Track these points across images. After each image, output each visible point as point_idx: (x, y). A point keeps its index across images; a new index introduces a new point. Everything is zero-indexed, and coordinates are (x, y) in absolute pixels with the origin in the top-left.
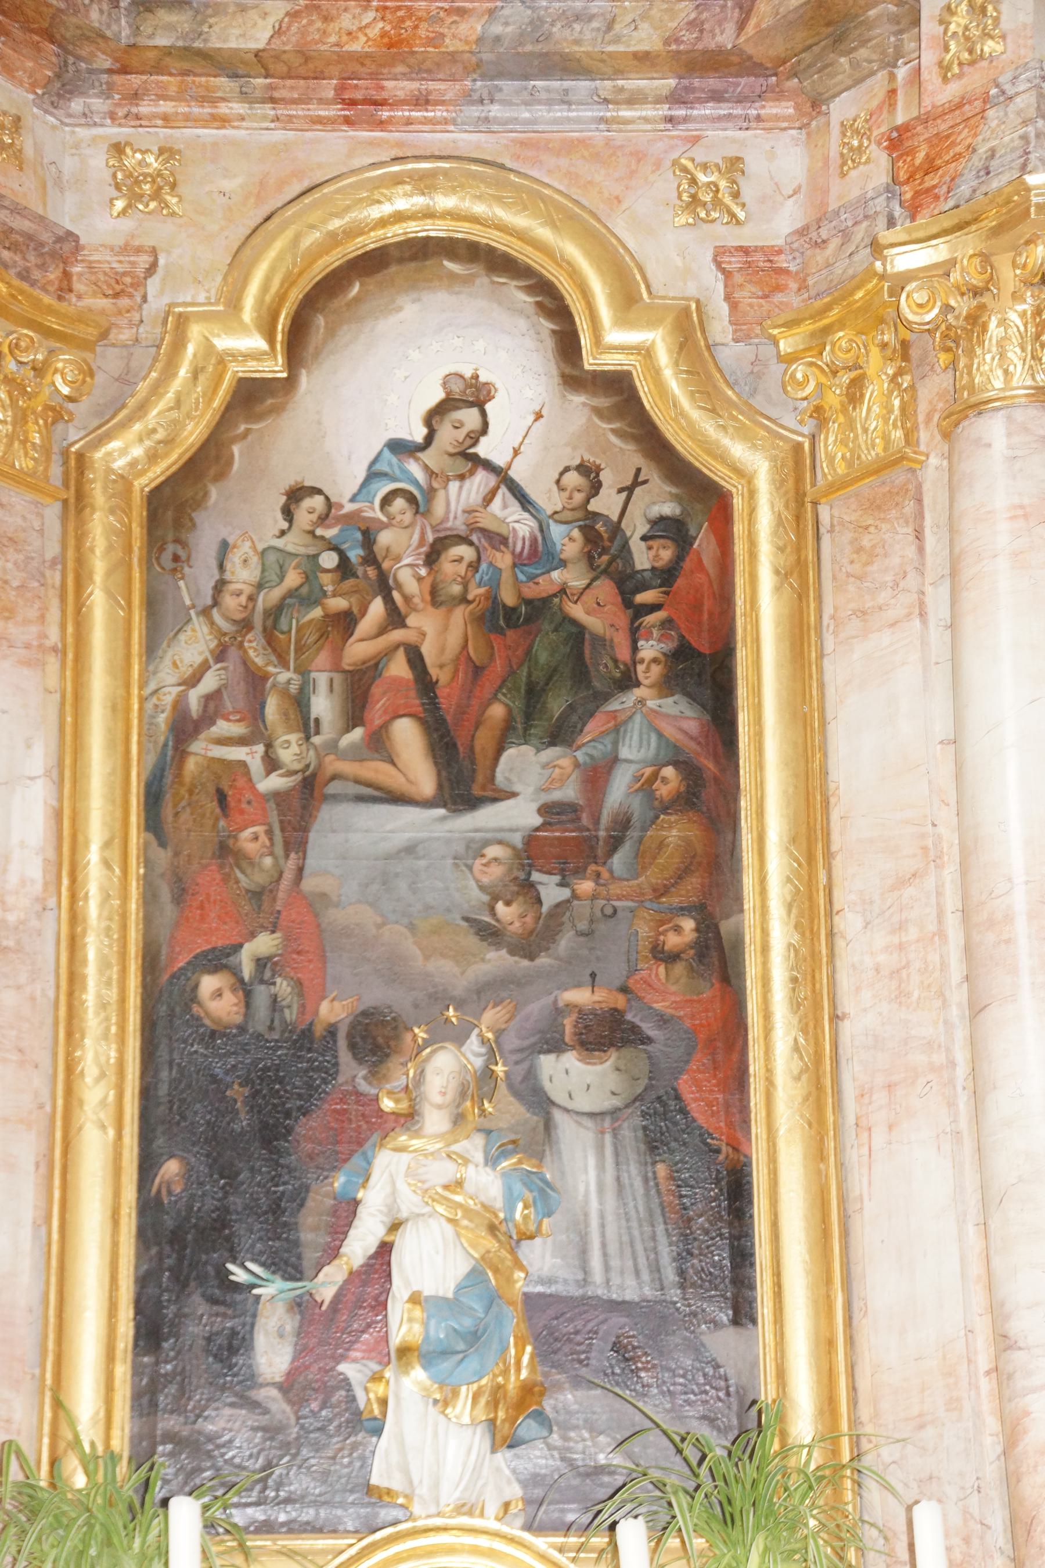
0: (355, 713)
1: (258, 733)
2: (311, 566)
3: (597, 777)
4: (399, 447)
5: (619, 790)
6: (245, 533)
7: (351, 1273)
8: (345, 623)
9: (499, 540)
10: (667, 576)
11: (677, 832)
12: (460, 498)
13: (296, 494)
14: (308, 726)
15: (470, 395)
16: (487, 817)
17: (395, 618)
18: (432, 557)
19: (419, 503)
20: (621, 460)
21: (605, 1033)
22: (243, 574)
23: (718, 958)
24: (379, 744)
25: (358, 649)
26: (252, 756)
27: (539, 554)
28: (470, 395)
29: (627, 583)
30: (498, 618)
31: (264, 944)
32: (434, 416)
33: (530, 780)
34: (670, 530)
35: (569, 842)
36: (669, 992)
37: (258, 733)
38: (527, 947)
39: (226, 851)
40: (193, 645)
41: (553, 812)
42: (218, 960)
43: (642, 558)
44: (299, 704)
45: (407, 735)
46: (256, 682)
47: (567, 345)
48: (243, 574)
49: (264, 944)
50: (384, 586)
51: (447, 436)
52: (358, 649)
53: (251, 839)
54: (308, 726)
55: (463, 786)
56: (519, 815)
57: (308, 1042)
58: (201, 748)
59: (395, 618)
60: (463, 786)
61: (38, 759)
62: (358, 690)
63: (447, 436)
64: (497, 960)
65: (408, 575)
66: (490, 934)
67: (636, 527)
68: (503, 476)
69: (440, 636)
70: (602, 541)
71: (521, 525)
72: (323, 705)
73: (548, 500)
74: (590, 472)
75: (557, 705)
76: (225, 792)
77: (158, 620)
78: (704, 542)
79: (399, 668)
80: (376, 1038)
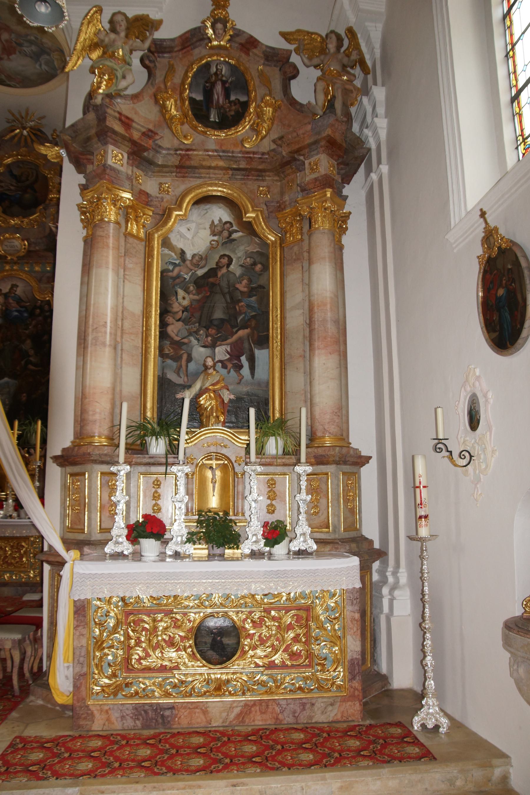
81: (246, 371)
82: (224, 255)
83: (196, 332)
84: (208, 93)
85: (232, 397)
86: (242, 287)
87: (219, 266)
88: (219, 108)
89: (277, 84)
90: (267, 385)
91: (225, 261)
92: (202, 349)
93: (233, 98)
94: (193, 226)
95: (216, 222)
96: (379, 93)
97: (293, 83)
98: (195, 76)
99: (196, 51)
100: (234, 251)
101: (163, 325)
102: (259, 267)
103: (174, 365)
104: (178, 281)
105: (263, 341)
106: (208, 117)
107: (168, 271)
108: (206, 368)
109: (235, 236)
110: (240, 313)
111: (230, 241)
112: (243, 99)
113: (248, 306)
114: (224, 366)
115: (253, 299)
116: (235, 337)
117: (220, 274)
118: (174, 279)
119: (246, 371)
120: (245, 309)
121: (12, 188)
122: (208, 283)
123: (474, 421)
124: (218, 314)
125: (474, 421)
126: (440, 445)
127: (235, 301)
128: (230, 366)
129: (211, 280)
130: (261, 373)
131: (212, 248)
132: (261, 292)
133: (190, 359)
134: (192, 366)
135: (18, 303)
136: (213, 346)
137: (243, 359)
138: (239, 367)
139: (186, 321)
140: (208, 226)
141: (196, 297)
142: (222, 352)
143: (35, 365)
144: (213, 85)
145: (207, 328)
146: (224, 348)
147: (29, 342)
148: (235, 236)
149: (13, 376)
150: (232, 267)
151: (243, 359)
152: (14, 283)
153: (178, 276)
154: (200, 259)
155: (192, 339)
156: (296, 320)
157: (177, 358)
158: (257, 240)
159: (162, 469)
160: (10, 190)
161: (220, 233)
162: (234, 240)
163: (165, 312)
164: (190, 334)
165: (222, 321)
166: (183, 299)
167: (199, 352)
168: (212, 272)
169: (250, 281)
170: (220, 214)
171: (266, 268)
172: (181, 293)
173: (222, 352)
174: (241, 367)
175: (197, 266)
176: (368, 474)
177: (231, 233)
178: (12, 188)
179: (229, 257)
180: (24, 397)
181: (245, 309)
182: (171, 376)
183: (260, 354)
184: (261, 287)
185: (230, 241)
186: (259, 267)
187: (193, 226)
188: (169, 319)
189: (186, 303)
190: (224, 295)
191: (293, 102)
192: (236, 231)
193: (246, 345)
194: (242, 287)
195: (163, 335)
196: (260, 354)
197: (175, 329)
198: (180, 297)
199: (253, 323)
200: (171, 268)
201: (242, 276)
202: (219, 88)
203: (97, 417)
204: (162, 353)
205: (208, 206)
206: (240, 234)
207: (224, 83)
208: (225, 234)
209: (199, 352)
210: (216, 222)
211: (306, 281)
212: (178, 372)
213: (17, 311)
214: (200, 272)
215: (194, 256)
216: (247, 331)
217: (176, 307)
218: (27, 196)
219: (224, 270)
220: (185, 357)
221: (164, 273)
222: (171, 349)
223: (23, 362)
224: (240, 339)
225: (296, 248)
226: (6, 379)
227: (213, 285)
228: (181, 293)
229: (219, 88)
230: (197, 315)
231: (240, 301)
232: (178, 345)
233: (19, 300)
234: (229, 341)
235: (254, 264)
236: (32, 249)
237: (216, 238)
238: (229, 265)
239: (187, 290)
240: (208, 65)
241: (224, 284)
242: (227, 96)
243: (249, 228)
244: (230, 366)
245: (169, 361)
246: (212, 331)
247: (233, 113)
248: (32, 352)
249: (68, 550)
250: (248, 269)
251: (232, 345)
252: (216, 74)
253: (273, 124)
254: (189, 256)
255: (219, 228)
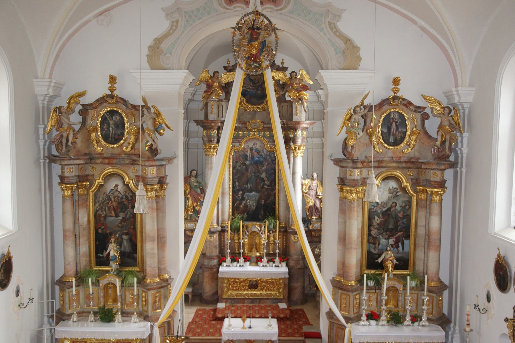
0: (109, 210)
1: (102, 212)
2: (106, 199)
3: (126, 215)
4: (112, 190)
5: (128, 216)
6: (101, 197)
7: (197, 125)
8: (108, 203)
9: (119, 197)
10: (131, 200)
11: (132, 219)
12: (116, 193)
13: (104, 193)
14: (106, 211)
15: (117, 186)
16: (119, 218)
17: (112, 203)
18: (114, 198)
19: (113, 194)
20: (128, 191)
21: (126, 234)
22: (101, 199)
23: (135, 229)
24: (111, 213)
25: (109, 205)
26: (102, 213)
27: (122, 198)
28: (117, 186)
29: (128, 200)
30: (119, 203)
31: (103, 227)
32: (114, 187)
33: (121, 216)
34: (131, 196)
35: (124, 220)
36: (131, 231)
37: (102, 212)
38: (121, 228)
39: (100, 220)
40: (97, 205)
41: (123, 218)
42: (100, 228)
43: (130, 199)
44: (105, 209)
45: (113, 212)
46: (102, 208)
47: (124, 182)
48: (101, 199)
49: (103, 227)
50: (111, 200)
51: (115, 189)
52: (109, 205)
53: (102, 219)
54: (106, 211)
55: (117, 216)
56: (121, 218)
57: (106, 234)
58: (98, 213)
59: (112, 203)
60: (117, 216)
61: (86, 215)
62: (109, 208)
63: (115, 189)
64: (119, 229)
65: (113, 200)
66: (119, 226)
67: (129, 196)
68: (119, 192)
69: (115, 204)
70: (127, 197)
71: (121, 196)
72: (107, 209)
73: (123, 194)
74: (126, 192)
75: (123, 210)
76: (100, 215)
77: (95, 203)
78: (134, 198)
79: (112, 207)
80: (111, 234)
81: (400, 249)
82: (394, 202)
83: (382, 233)
84: (389, 128)
85: (397, 263)
86: (400, 215)
87: (391, 207)
88: (394, 135)
89: (419, 120)
90: (408, 253)
91: (394, 204)
92: (384, 240)
93: (400, 130)
94: (382, 190)
95: (391, 188)
96: (465, 135)
97: (426, 121)
98: (384, 120)
99: (384, 107)
100: (398, 200)
101: (369, 230)
102: (407, 207)
103: (373, 246)
104: (375, 213)
105: (408, 237)
106: (389, 140)
107: (372, 209)
108: (387, 250)
109: (398, 194)
110: (399, 226)
111: (396, 196)
112: (404, 130)
113: (402, 223)
114: (392, 247)
115: (405, 220)
116: (397, 235)
117: (392, 210)
118: (374, 212)
119: (400, 249)
120: (401, 224)
121: (251, 87)
122: (387, 214)
123: (489, 299)
124: (391, 226)
125: (489, 299)
126: (476, 306)
127: (397, 221)
128: (394, 246)
129: (388, 212)
130: (406, 249)
131: (389, 199)
132: (408, 217)
133: (379, 244)
134: (380, 247)
135: (257, 153)
136: (388, 239)
137: (400, 244)
138: (398, 247)
139: (378, 229)
140: (388, 190)
141: (382, 220)
142: (391, 241)
143: (268, 186)
144: (392, 124)
145: (386, 232)
146: (392, 239)
147: (264, 173)
148: (398, 194)
149: (257, 191)
150: (397, 207)
151: (400, 244)
152: (255, 142)
153: (376, 211)
154: (384, 204)
155: (380, 236)
156: (421, 231)
157: (374, 244)
158: (407, 195)
159: (374, 291)
160: (249, 88)
161: (392, 193)
162: (398, 196)
163: (370, 225)
164: (380, 234)
165: (392, 229)
166: (377, 220)
167: (383, 241)
168: (389, 209)
169: (404, 213)
170: (393, 184)
171: (410, 207)
172: (377, 218)
173: (391, 241)
174: (399, 247)
175: (383, 207)
176: (446, 293)
177: (397, 193)
178: (251, 87)
179: (396, 203)
180: (263, 202)
181: (401, 224)
182: (372, 250)
183: (406, 242)
184: (408, 215)
185: (396, 196)
186: (407, 207)
187: (382, 190)
188: (372, 228)
189: (378, 222)
190: (393, 218)
191: (426, 133)
192: (399, 192)
193: (401, 238)
194: (400, 215)
195: (369, 234)
196: (406, 242)
197: (374, 232)
198: (376, 220)
199: (404, 230)
200: (373, 207)
201: (401, 210)
202: (394, 125)
203: (352, 275)
204: (369, 242)
205: (388, 181)
206: (401, 193)
207: (396, 122)
208: (395, 193)
209: (383, 241)
210: (391, 188)
211: (428, 217)
212: (375, 249)
213: (257, 157)
214: (384, 209)
215: (382, 203)
216: (402, 233)
217: (375, 224)
218: (259, 92)
219: (394, 208)
220: (378, 243)
221: (370, 211)
222: (372, 240)
223: (262, 184)
224: (399, 236)
225: (423, 202)
226: (253, 193)
227: (389, 214)
228: (377, 218)
229: (394, 125)
230: (383, 227)
231: (399, 221)
232: (375, 238)
233: (258, 152)
234: (395, 237)
235: (406, 206)
236: (265, 126)
237: (391, 195)
238: (395, 206)
239: (379, 217)
240: (390, 113)
241: (393, 214)
242: (397, 130)
243: (404, 190)
244: (394, 246)
245: (371, 245)
246: (388, 233)
247: (399, 137)
248: (266, 179)
249: (347, 323)
250: (403, 208)
251: (396, 238)
252: (393, 118)
253: (416, 142)
254: (380, 203)
255: (392, 191)
